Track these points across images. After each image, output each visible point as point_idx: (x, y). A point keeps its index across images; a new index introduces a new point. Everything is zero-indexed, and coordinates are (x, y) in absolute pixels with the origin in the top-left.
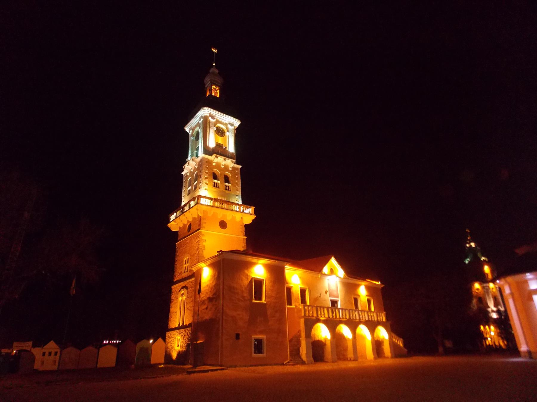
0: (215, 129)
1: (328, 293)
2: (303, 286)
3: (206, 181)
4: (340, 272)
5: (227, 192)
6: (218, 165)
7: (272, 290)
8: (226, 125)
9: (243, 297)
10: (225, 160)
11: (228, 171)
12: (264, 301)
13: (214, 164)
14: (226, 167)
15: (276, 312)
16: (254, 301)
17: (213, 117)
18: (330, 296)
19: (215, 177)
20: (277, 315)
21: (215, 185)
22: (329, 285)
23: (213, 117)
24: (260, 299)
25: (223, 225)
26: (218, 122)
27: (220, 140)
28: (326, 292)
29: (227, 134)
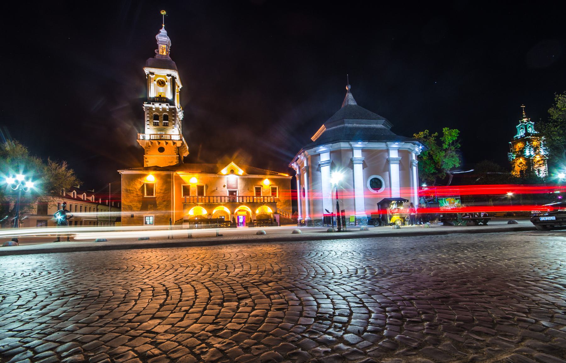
0: (156, 82)
1: (226, 187)
2: (199, 184)
3: (148, 123)
4: (241, 172)
5: (165, 127)
6: (157, 109)
7: (161, 190)
8: (164, 77)
9: (137, 195)
10: (160, 105)
11: (166, 111)
12: (154, 196)
13: (154, 110)
14: (164, 110)
15: (164, 201)
16: (146, 196)
17: (153, 74)
18: (228, 188)
19: (156, 117)
20: (165, 203)
21: (156, 124)
22: (227, 181)
23: (153, 74)
24: (153, 195)
25: (161, 150)
26: (157, 76)
27: (161, 89)
28: (224, 186)
29: (166, 83)
